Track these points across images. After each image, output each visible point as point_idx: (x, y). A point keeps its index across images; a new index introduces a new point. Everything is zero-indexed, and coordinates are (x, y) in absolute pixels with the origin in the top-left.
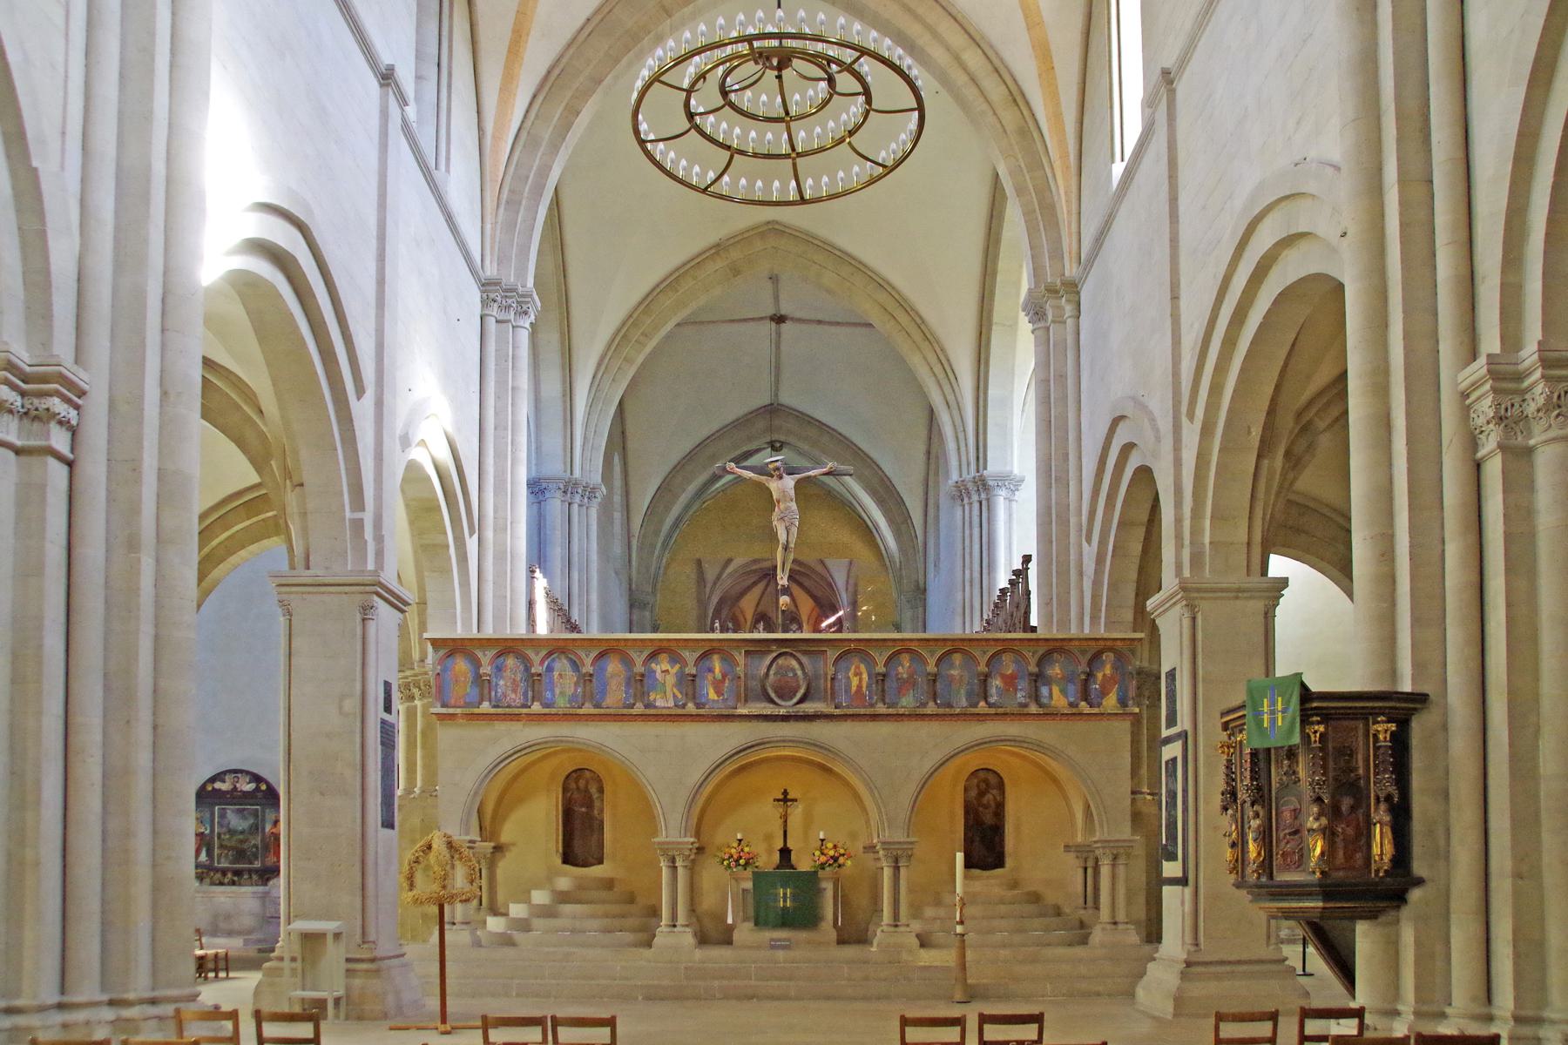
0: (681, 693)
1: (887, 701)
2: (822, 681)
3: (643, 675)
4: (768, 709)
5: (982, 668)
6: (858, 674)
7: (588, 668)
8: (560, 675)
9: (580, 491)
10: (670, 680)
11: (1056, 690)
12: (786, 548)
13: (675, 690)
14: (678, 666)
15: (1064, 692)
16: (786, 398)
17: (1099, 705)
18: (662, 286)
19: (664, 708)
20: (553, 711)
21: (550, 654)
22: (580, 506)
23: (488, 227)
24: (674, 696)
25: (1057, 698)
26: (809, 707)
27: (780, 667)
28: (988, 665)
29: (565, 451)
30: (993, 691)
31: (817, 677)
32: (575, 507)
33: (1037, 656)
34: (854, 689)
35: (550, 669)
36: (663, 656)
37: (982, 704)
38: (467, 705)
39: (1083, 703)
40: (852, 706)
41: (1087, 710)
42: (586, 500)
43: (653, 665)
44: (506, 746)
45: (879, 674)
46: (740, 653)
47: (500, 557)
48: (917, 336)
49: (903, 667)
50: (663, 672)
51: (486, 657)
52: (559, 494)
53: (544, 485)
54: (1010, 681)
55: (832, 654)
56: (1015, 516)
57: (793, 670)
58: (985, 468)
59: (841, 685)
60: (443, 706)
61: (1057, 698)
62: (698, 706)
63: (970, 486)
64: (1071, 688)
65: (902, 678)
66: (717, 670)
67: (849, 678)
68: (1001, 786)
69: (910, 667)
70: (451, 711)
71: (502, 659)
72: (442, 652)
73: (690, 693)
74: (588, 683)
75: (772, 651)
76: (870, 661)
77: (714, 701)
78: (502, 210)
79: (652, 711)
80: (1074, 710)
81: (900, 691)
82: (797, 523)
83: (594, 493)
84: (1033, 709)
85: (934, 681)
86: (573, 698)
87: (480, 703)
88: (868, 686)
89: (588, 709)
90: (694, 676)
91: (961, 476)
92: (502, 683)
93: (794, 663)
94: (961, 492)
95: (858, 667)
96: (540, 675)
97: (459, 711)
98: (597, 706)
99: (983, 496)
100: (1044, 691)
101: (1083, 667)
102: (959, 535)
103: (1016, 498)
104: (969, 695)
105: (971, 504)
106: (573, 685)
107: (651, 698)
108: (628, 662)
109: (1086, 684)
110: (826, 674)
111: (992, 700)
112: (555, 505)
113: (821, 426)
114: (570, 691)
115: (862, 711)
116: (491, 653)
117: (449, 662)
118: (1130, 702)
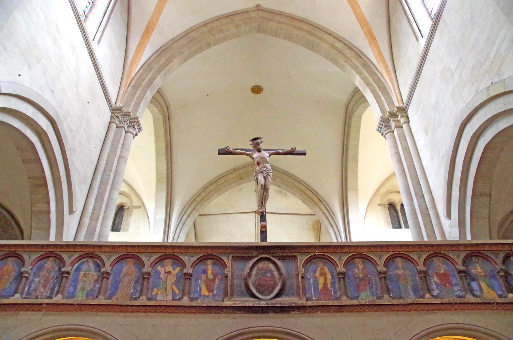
0: (179, 289)
1: (349, 295)
4: (250, 302)
6: (323, 274)
10: (172, 279)
11: (484, 285)
14: (178, 269)
21: (81, 257)
23: (121, 92)
24: (173, 291)
27: (261, 269)
28: (424, 264)
30: (434, 286)
34: (321, 286)
35: (78, 270)
40: (320, 300)
43: (159, 268)
46: (229, 258)
49: (358, 269)
50: (166, 273)
57: (271, 272)
65: (359, 277)
66: (210, 272)
67: (316, 277)
69: (363, 269)
71: (42, 262)
74: (105, 279)
75: (255, 257)
77: (205, 296)
78: (130, 88)
81: (358, 289)
88: (333, 283)
89: (102, 300)
92: (37, 280)
93: (271, 266)
95: (322, 269)
104: (415, 290)
106: (92, 282)
111: (435, 293)
115: (330, 303)
116: (35, 256)
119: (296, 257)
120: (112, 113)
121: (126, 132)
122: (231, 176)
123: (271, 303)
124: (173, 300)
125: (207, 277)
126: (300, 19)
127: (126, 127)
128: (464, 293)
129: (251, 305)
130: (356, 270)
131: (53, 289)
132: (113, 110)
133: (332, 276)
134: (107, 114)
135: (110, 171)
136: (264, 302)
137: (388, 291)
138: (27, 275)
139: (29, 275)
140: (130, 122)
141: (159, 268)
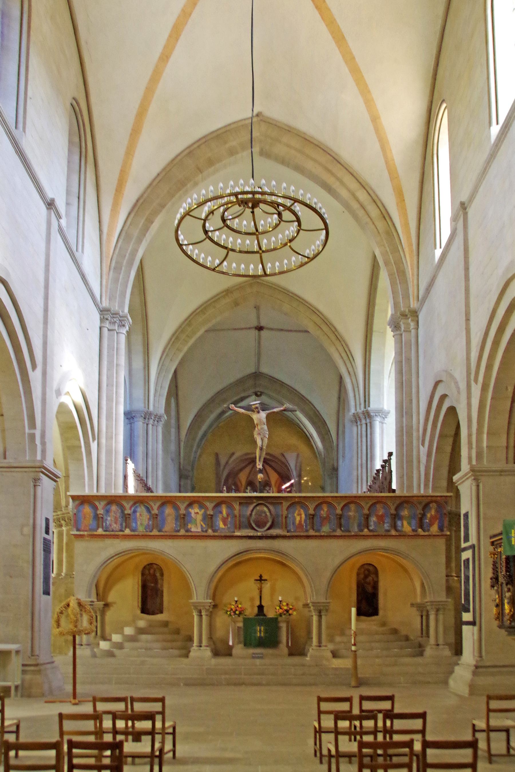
0: (205, 524)
2: (280, 519)
3: (184, 515)
4: (251, 533)
5: (366, 511)
6: (300, 515)
7: (155, 511)
8: (140, 515)
9: (153, 418)
10: (199, 517)
11: (405, 523)
12: (261, 449)
13: (202, 523)
14: (203, 511)
15: (409, 524)
16: (265, 369)
17: (428, 530)
18: (198, 311)
19: (196, 532)
20: (136, 533)
21: (135, 503)
22: (153, 425)
24: (202, 526)
25: (406, 527)
26: (274, 532)
29: (145, 396)
31: (278, 516)
32: (150, 426)
33: (395, 505)
35: (135, 512)
36: (196, 506)
37: (366, 530)
38: (90, 530)
39: (420, 530)
41: (422, 533)
42: (156, 422)
43: (190, 510)
44: (111, 551)
45: (311, 515)
47: (109, 452)
48: (333, 338)
51: (101, 505)
52: (141, 420)
53: (133, 415)
54: (381, 519)
55: (285, 504)
56: (385, 431)
57: (265, 512)
58: (369, 406)
59: (290, 521)
60: (78, 530)
61: (406, 527)
62: (214, 531)
63: (361, 416)
64: (414, 522)
67: (295, 516)
68: (376, 572)
70: (82, 533)
72: (77, 502)
73: (210, 524)
74: (155, 519)
76: (305, 508)
77: (222, 528)
79: (190, 534)
80: (415, 533)
81: (322, 525)
82: (267, 436)
83: (160, 418)
84: (393, 533)
85: (340, 518)
86: (147, 527)
87: (97, 529)
90: (212, 515)
91: (356, 410)
92: (109, 518)
93: (265, 509)
94: (356, 419)
95: (299, 511)
96: (129, 515)
97: (86, 533)
98: (159, 531)
99: (368, 421)
100: (399, 523)
101: (419, 511)
102: (355, 441)
103: (385, 422)
104: (359, 526)
105: (361, 425)
106: (147, 520)
107: (189, 527)
108: (177, 508)
109: (421, 520)
110: (282, 515)
111: (371, 528)
112: (139, 425)
113: (282, 384)
114: (145, 523)
115: (302, 534)
116: (103, 503)
117: (81, 508)
118: (445, 529)
119: (282, 503)
120: (100, 315)
121: (117, 333)
122: (223, 302)
123: (264, 534)
124: (202, 531)
125: (223, 517)
126: (316, 143)
127: (116, 328)
128: (390, 528)
129: (252, 535)
130: (322, 512)
131: (121, 525)
132: (101, 311)
133: (306, 515)
134: (96, 316)
135: (113, 386)
136: (260, 534)
137: (340, 526)
138: (102, 516)
139: (103, 515)
140: (119, 320)
141: (190, 510)
